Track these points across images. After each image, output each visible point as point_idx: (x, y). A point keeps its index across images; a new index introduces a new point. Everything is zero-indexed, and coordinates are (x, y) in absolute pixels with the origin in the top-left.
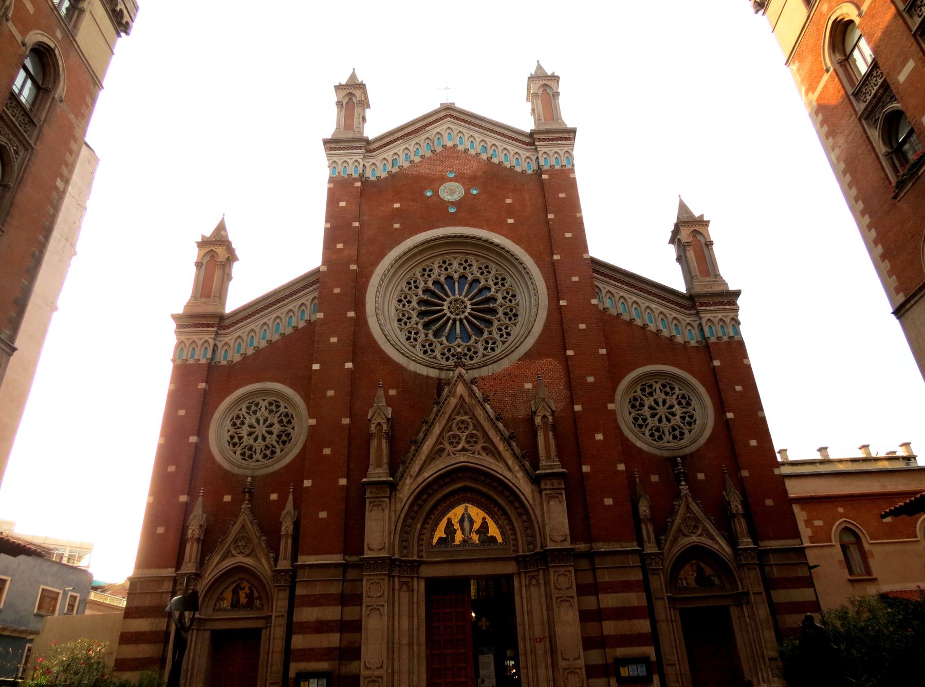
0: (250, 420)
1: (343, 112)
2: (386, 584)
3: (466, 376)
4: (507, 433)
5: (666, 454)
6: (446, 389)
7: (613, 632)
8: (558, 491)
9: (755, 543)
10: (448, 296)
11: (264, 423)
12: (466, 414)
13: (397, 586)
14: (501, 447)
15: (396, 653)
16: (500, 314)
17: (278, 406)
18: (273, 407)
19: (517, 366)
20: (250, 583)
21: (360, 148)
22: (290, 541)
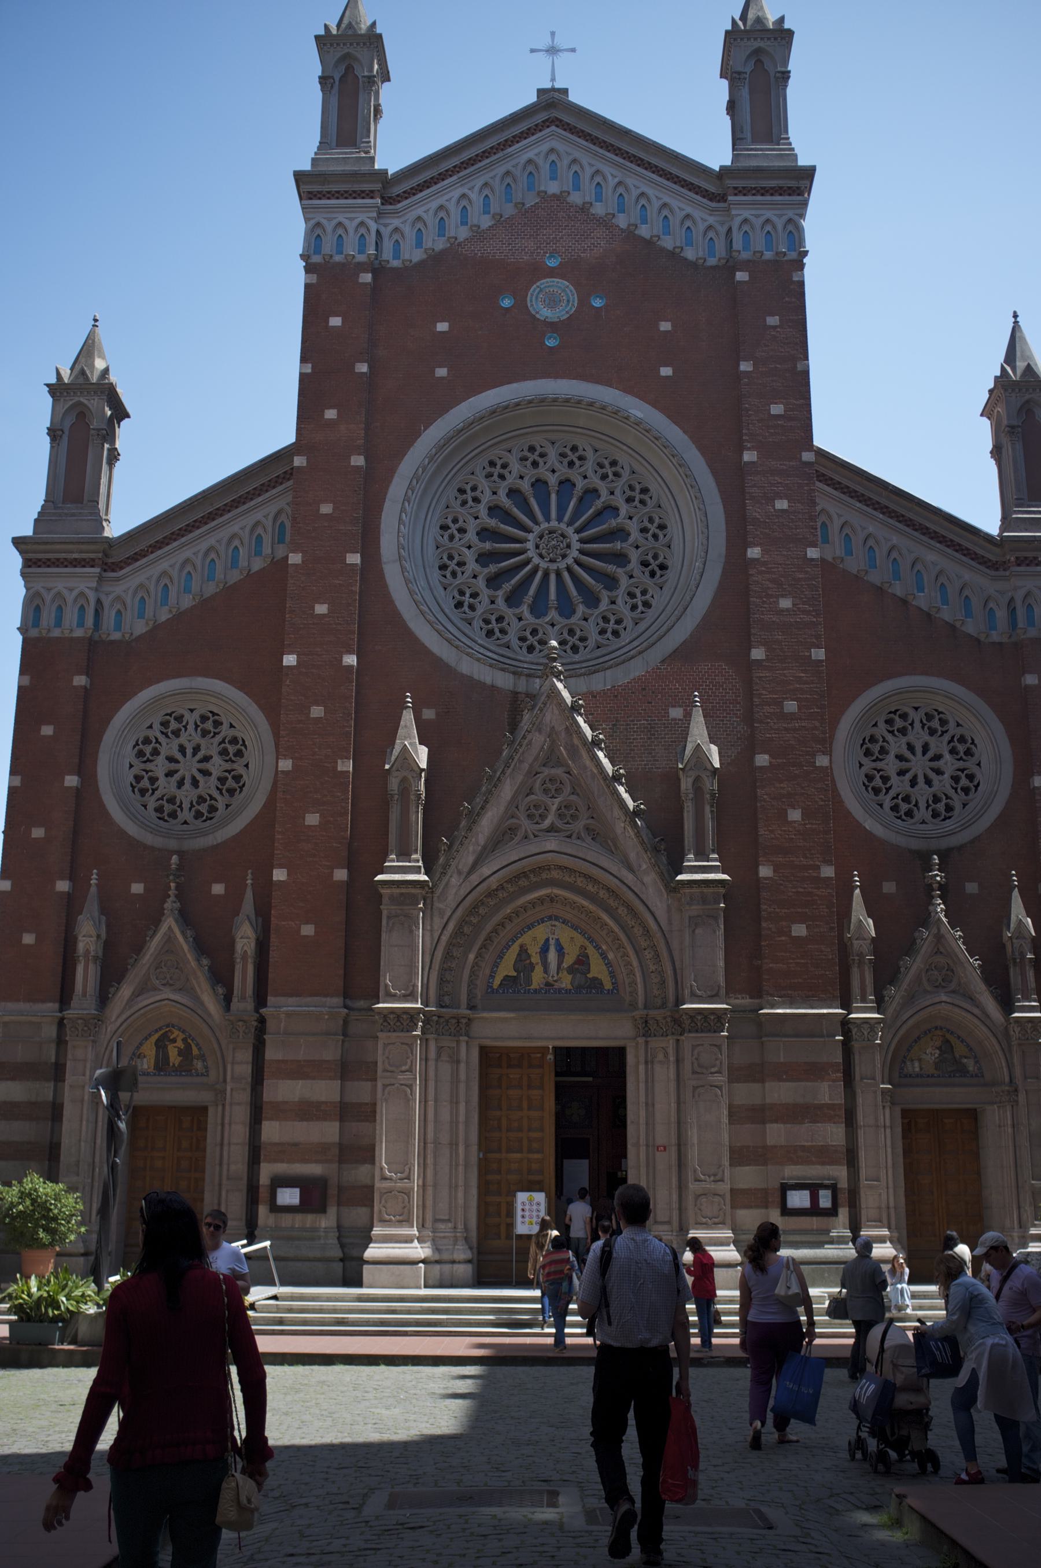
1: (334, 101)
5: (915, 844)
6: (527, 717)
10: (537, 523)
11: (194, 754)
13: (432, 1054)
18: (209, 725)
20: (183, 1032)
21: (370, 194)
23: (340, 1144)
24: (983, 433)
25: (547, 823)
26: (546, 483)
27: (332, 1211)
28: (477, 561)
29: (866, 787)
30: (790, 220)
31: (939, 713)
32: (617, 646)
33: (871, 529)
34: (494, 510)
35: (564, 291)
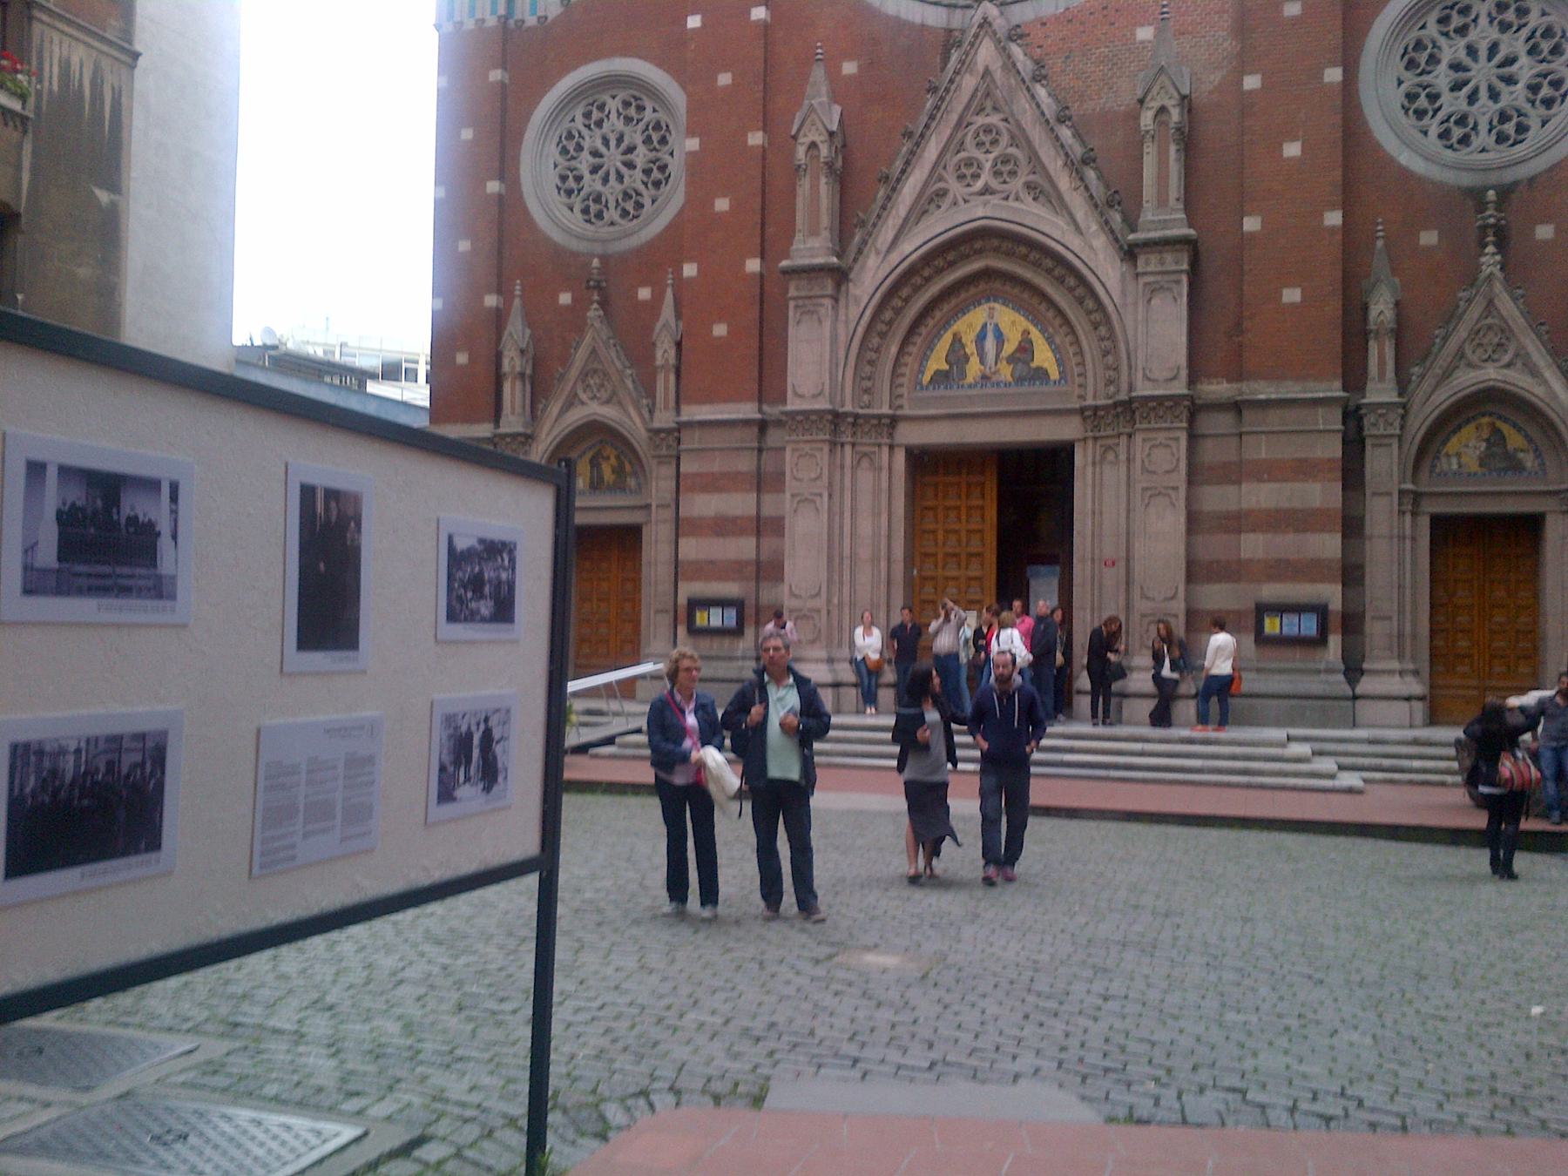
0: (592, 140)
2: (826, 457)
3: (1000, 24)
4: (1078, 151)
5: (1467, 180)
6: (955, 56)
7: (1260, 554)
8: (1173, 277)
11: (618, 146)
14: (1064, 182)
15: (847, 573)
17: (641, 109)
18: (632, 112)
22: (672, 378)
23: (758, 563)
25: (979, 184)
27: (749, 632)
29: (1407, 111)
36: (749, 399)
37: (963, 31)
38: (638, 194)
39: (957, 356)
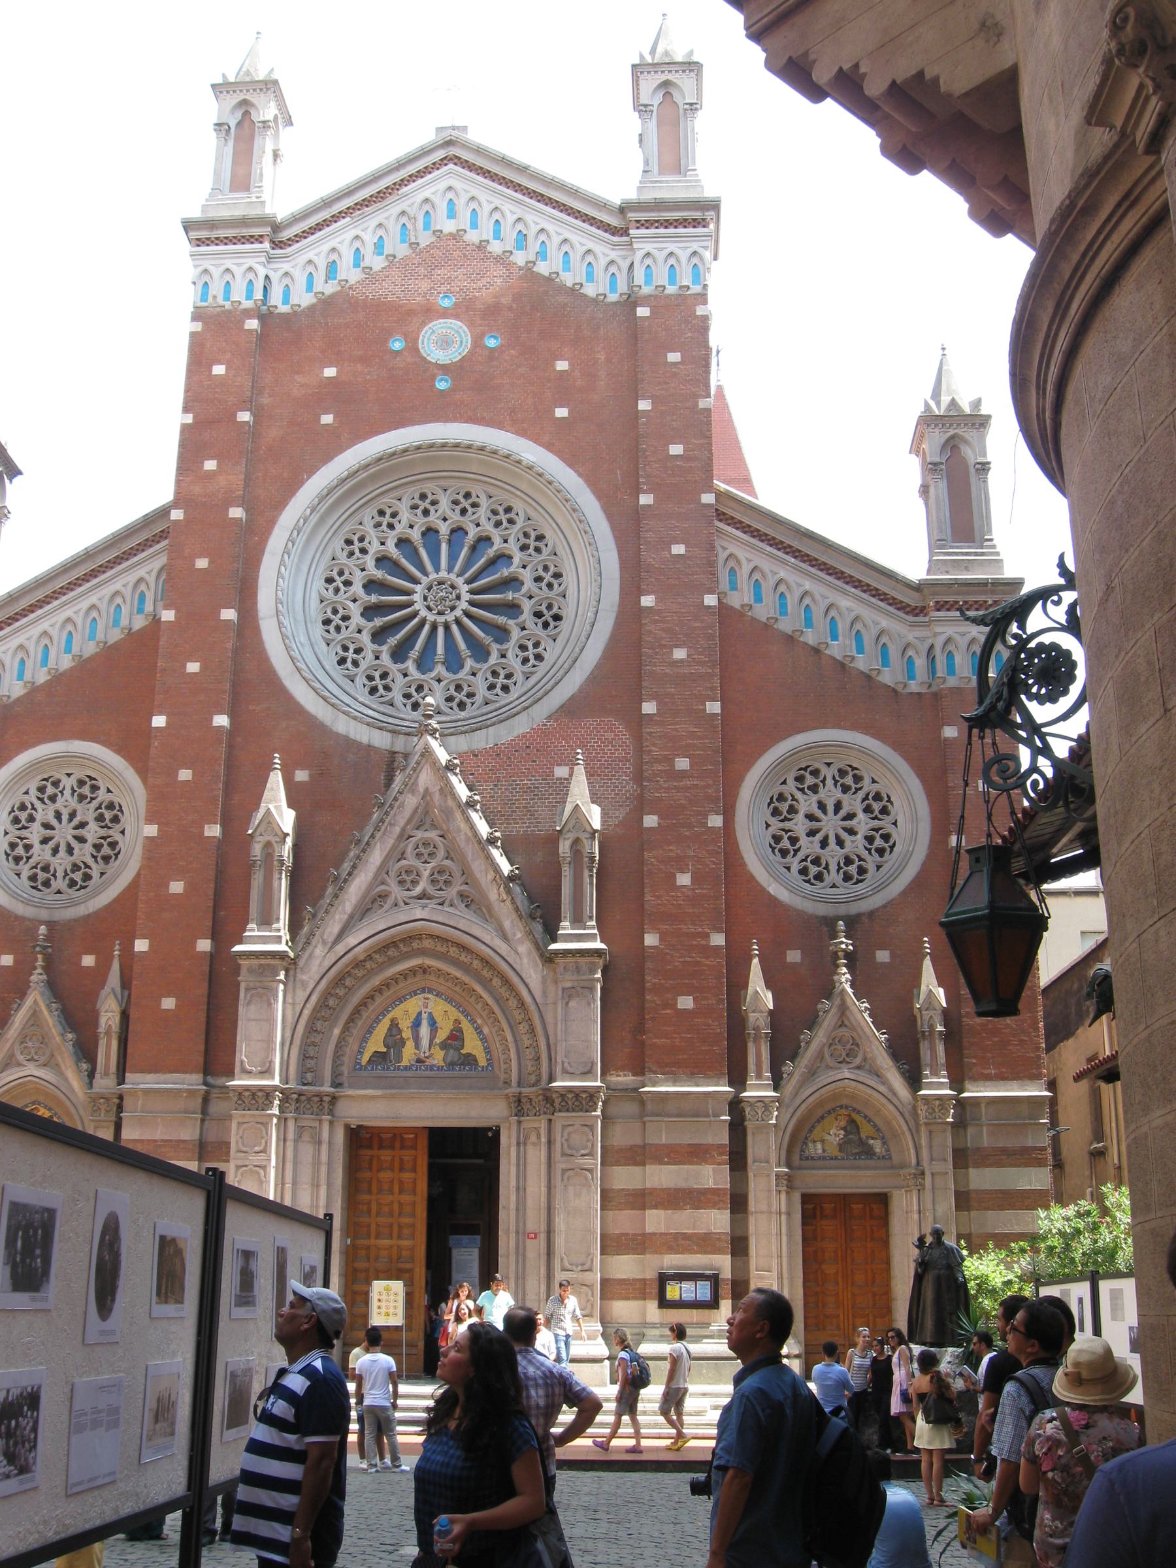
5: (822, 910)
6: (399, 779)
9: (957, 1083)
10: (426, 574)
11: (70, 820)
12: (434, 826)
13: (291, 1135)
16: (527, 616)
18: (86, 790)
19: (541, 732)
21: (259, 239)
24: (912, 471)
26: (437, 532)
28: (362, 615)
29: (773, 849)
30: (695, 253)
31: (854, 769)
32: (507, 701)
33: (782, 574)
34: (382, 560)
35: (458, 332)
36: (198, 1072)
37: (406, 756)
38: (87, 866)
39: (394, 1039)
